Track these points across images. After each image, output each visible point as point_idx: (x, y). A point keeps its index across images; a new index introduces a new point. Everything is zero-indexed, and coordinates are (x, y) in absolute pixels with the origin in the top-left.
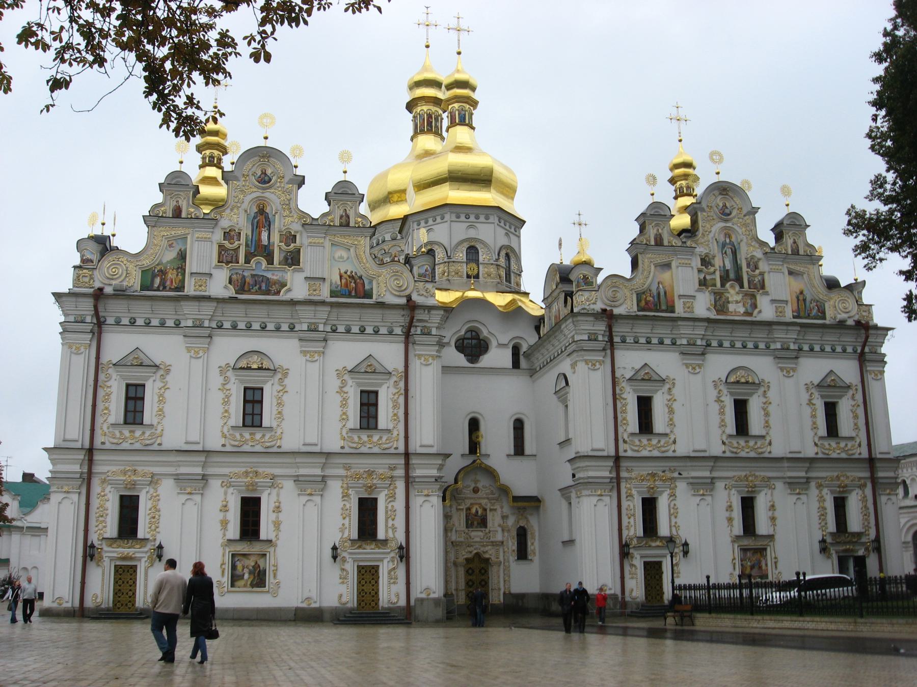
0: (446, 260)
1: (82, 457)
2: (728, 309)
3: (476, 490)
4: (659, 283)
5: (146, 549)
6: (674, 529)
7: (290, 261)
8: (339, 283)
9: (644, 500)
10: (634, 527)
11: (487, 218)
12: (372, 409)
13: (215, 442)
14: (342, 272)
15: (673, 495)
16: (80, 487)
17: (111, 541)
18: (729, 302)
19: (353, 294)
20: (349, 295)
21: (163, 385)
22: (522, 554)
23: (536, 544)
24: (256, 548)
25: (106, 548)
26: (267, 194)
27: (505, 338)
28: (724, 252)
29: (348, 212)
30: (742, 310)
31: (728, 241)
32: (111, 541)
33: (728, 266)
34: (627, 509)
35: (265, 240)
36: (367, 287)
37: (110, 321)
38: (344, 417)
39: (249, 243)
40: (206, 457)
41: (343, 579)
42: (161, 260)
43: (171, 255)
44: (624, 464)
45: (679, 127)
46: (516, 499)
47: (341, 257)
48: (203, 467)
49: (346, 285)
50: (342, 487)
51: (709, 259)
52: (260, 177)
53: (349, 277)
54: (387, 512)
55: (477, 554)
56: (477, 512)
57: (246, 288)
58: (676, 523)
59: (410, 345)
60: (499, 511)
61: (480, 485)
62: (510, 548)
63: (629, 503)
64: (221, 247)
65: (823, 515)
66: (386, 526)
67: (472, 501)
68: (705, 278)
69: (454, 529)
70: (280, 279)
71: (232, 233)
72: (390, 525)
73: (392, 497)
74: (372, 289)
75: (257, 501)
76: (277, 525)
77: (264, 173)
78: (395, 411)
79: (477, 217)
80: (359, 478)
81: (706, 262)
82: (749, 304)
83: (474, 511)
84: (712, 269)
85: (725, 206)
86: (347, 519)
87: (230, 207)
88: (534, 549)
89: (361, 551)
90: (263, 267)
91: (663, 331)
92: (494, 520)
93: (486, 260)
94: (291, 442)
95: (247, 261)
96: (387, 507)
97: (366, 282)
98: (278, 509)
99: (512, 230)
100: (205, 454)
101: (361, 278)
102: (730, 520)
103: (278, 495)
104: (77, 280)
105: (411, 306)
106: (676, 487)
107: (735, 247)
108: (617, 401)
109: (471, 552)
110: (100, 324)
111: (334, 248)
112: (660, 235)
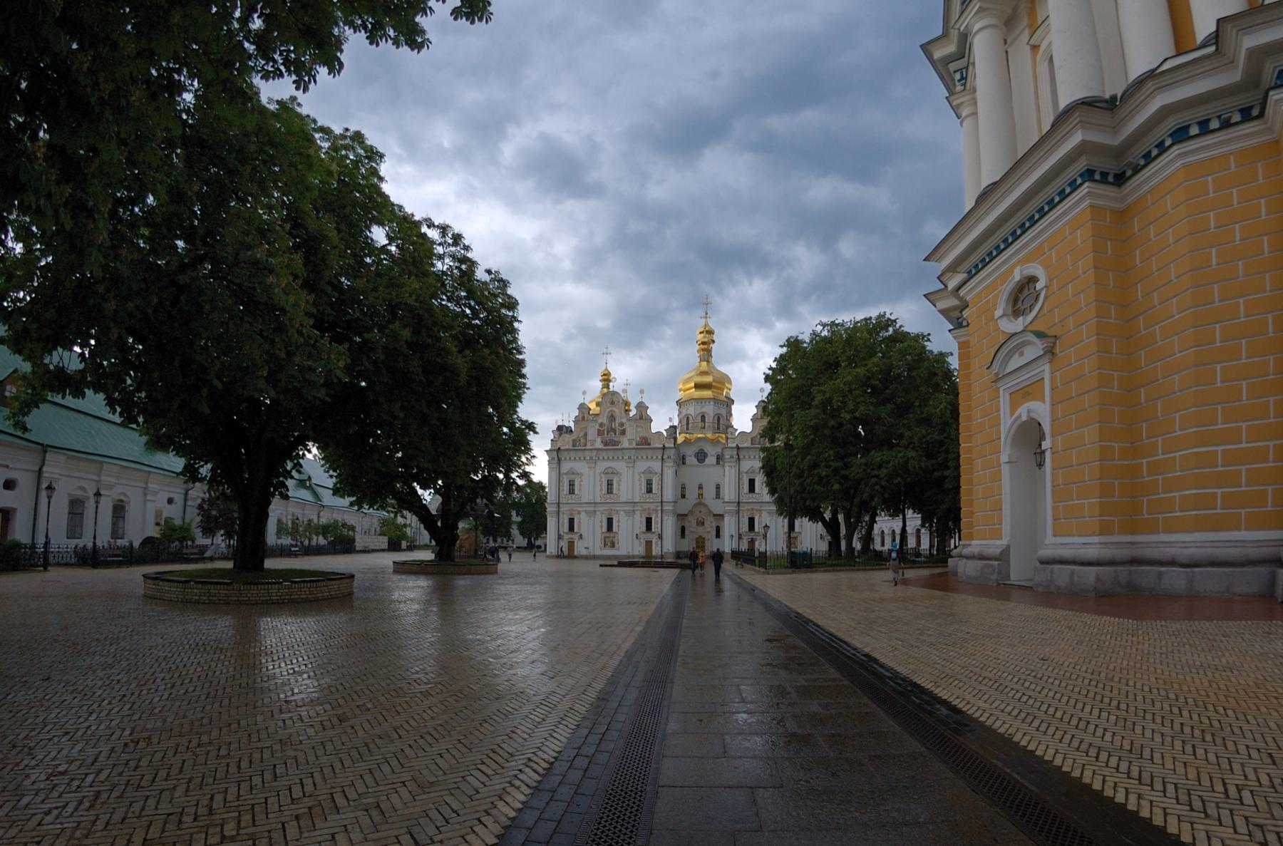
3: (700, 512)
9: (750, 519)
10: (745, 527)
13: (598, 500)
15: (760, 516)
17: (566, 533)
22: (718, 535)
24: (612, 535)
26: (614, 409)
27: (713, 453)
32: (566, 533)
38: (641, 489)
41: (640, 546)
43: (582, 434)
44: (741, 504)
46: (714, 515)
64: (599, 430)
73: (657, 516)
75: (612, 519)
76: (619, 526)
92: (707, 523)
94: (623, 499)
98: (619, 522)
102: (783, 526)
104: (552, 444)
105: (664, 448)
110: (559, 460)
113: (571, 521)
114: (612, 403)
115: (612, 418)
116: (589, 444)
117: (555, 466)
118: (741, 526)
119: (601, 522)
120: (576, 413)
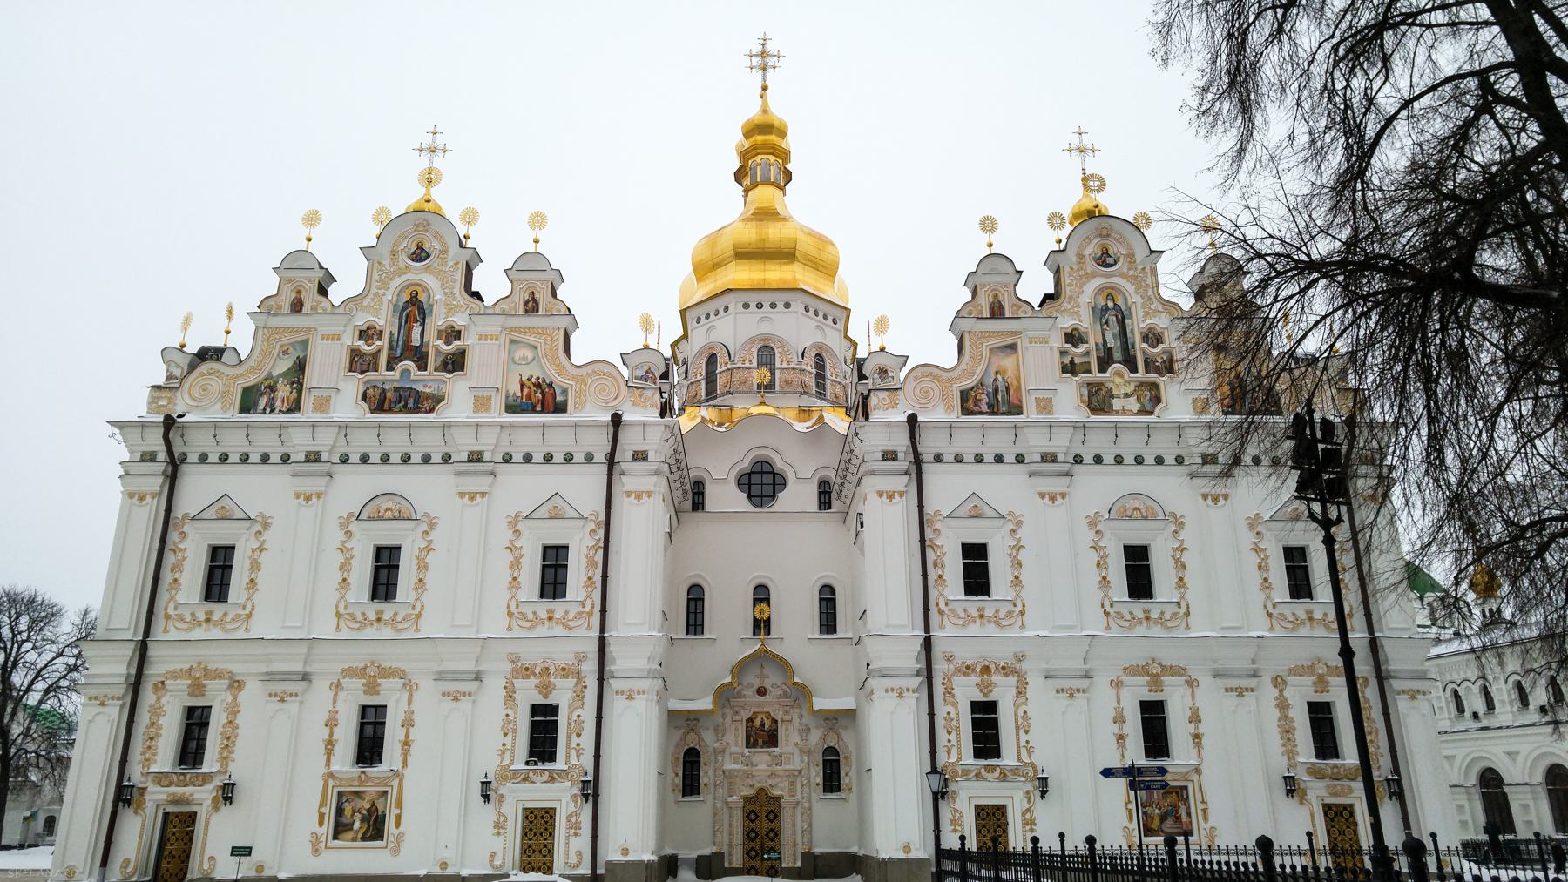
0: (729, 366)
1: (130, 652)
2: (1111, 406)
3: (762, 692)
4: (997, 373)
5: (209, 787)
6: (1024, 752)
7: (450, 366)
8: (519, 394)
9: (976, 706)
10: (959, 746)
11: (787, 305)
12: (560, 571)
14: (524, 378)
16: (124, 696)
18: (1112, 396)
19: (538, 409)
20: (534, 411)
21: (258, 545)
23: (853, 773)
25: (151, 787)
28: (1104, 321)
29: (537, 296)
30: (1136, 407)
31: (1111, 304)
33: (1112, 342)
34: (945, 718)
35: (416, 341)
36: (559, 398)
37: (193, 457)
39: (395, 344)
40: (310, 648)
42: (270, 373)
43: (285, 365)
45: (1083, 162)
47: (524, 358)
48: (305, 662)
49: (529, 397)
50: (505, 688)
51: (1079, 334)
52: (414, 253)
53: (534, 385)
54: (569, 724)
55: (762, 789)
56: (763, 724)
57: (386, 406)
58: (1027, 742)
59: (615, 478)
60: (796, 721)
61: (767, 684)
62: (812, 780)
63: (950, 709)
65: (1287, 732)
66: (568, 747)
67: (754, 710)
68: (1072, 362)
69: (727, 750)
70: (435, 393)
71: (371, 332)
72: (573, 745)
74: (566, 401)
75: (381, 709)
76: (406, 744)
77: (420, 248)
78: (590, 574)
79: (773, 306)
80: (528, 677)
81: (1073, 337)
82: (1148, 398)
83: (757, 723)
84: (1086, 346)
85: (1106, 253)
86: (510, 735)
87: (371, 296)
88: (850, 782)
89: (527, 785)
90: (412, 377)
91: (999, 441)
92: (789, 738)
93: (785, 363)
95: (390, 368)
96: (570, 718)
97: (558, 391)
98: (408, 723)
99: (830, 321)
100: (306, 644)
101: (550, 385)
103: (410, 703)
104: (153, 401)
106: (1027, 683)
107: (1122, 313)
108: (929, 552)
109: (752, 786)
111: (514, 346)
112: (999, 302)
113: (196, 723)
114: (420, 255)
115: (414, 309)
116: (307, 401)
117: (156, 484)
118: (940, 737)
119: (331, 723)
120: (270, 285)
